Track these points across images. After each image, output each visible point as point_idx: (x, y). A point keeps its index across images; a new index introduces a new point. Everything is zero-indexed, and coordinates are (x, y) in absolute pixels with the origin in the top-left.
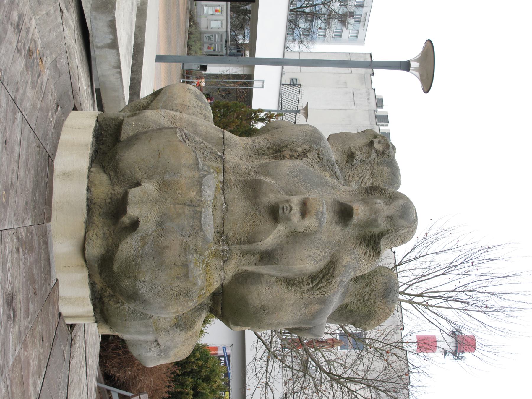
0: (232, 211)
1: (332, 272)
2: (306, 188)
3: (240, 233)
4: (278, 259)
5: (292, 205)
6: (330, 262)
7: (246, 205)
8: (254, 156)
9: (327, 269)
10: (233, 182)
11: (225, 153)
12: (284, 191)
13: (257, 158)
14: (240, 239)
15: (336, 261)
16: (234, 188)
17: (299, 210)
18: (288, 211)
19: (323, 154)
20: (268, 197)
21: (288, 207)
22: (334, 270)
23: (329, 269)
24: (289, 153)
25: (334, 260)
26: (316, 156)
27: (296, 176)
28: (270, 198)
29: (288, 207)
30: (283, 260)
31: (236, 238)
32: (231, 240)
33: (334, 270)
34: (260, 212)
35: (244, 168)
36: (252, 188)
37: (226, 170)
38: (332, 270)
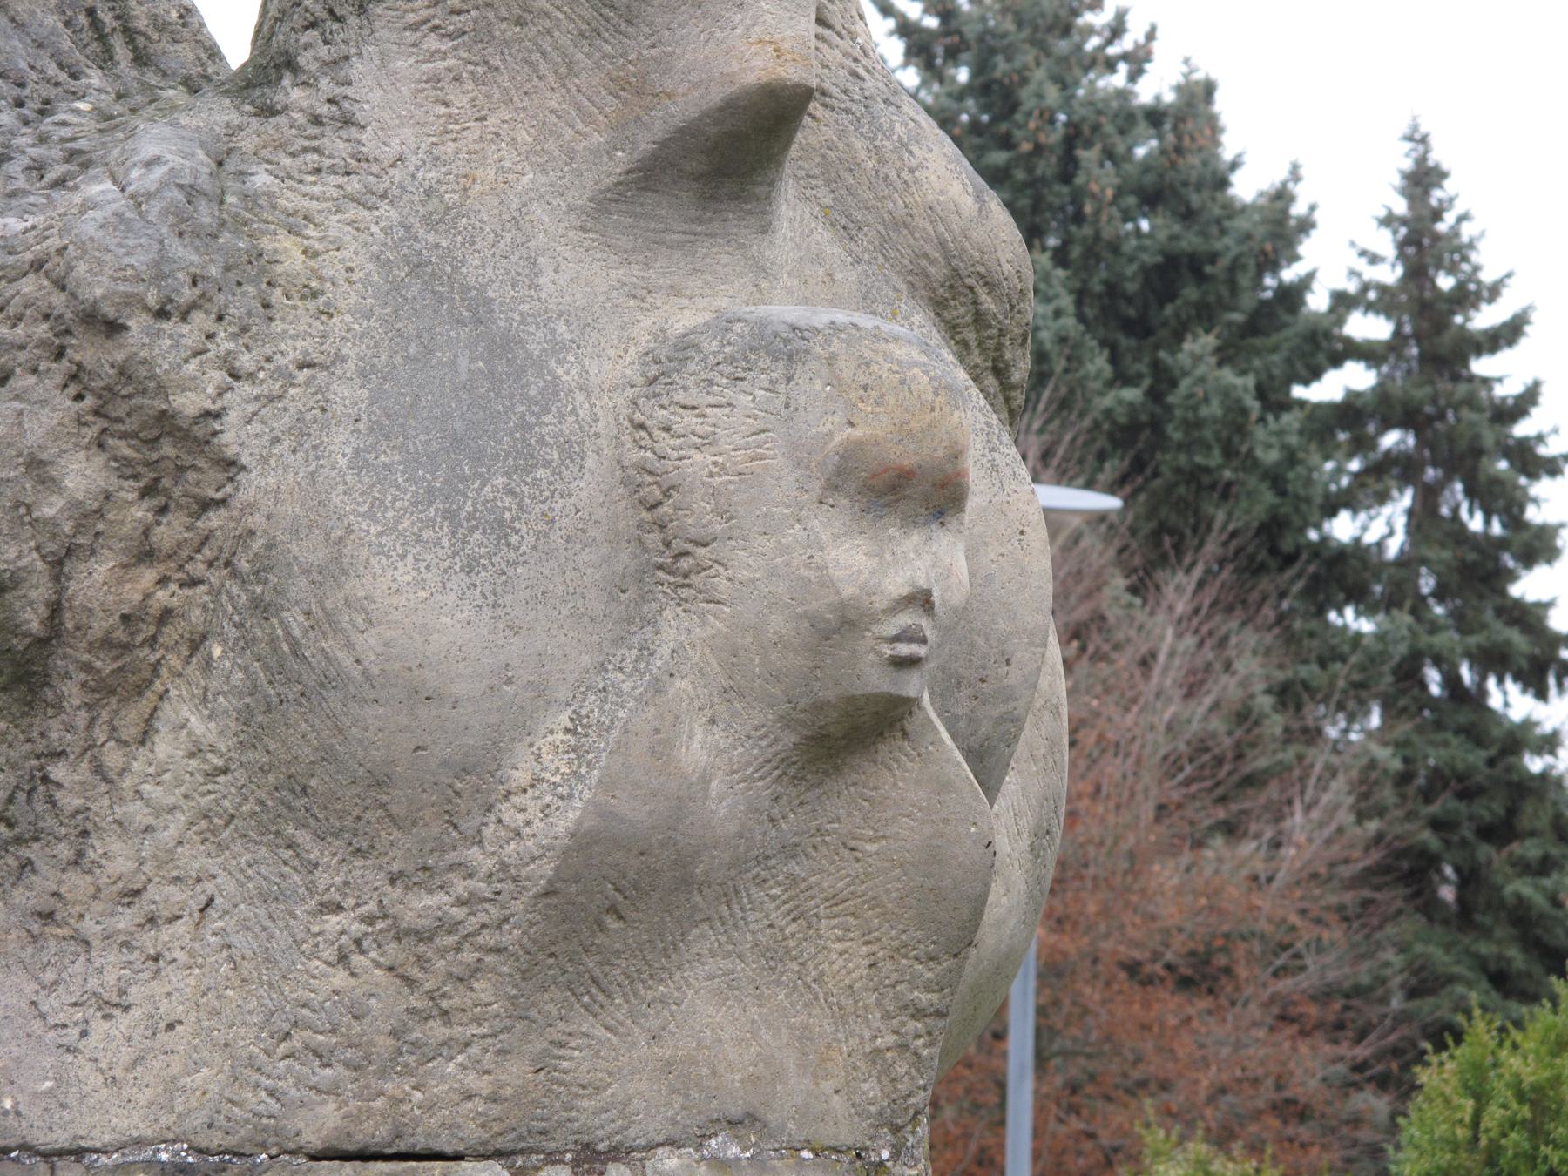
0: (754, 1080)
1: (999, 300)
2: (571, 452)
3: (875, 1017)
4: (1001, 720)
5: (896, 584)
6: (938, 306)
7: (711, 966)
8: (46, 879)
9: (971, 336)
10: (515, 1072)
11: (60, 1139)
12: (618, 642)
13: (65, 851)
14: (919, 1013)
15: (948, 258)
16: (576, 1063)
17: (916, 538)
18: (925, 622)
19: (159, 272)
20: (705, 779)
21: (905, 620)
22: (991, 286)
23: (980, 319)
24: (102, 568)
25: (938, 272)
26: (190, 332)
27: (501, 530)
28: (713, 758)
29: (905, 620)
30: (1014, 676)
31: (903, 1047)
32: (903, 1087)
33: (991, 286)
34: (790, 851)
35: (340, 978)
36: (618, 906)
37: (375, 1133)
38: (988, 302)
